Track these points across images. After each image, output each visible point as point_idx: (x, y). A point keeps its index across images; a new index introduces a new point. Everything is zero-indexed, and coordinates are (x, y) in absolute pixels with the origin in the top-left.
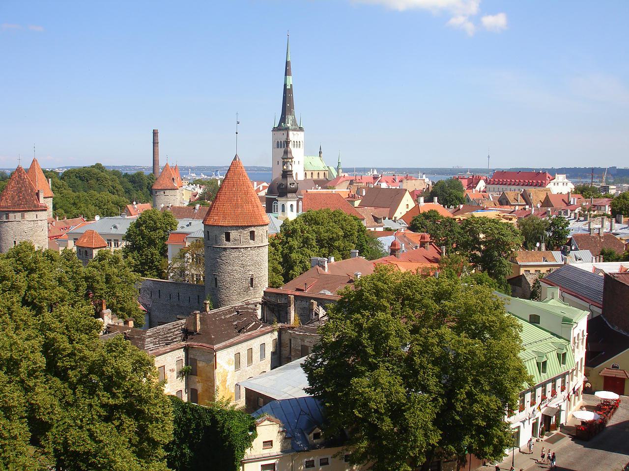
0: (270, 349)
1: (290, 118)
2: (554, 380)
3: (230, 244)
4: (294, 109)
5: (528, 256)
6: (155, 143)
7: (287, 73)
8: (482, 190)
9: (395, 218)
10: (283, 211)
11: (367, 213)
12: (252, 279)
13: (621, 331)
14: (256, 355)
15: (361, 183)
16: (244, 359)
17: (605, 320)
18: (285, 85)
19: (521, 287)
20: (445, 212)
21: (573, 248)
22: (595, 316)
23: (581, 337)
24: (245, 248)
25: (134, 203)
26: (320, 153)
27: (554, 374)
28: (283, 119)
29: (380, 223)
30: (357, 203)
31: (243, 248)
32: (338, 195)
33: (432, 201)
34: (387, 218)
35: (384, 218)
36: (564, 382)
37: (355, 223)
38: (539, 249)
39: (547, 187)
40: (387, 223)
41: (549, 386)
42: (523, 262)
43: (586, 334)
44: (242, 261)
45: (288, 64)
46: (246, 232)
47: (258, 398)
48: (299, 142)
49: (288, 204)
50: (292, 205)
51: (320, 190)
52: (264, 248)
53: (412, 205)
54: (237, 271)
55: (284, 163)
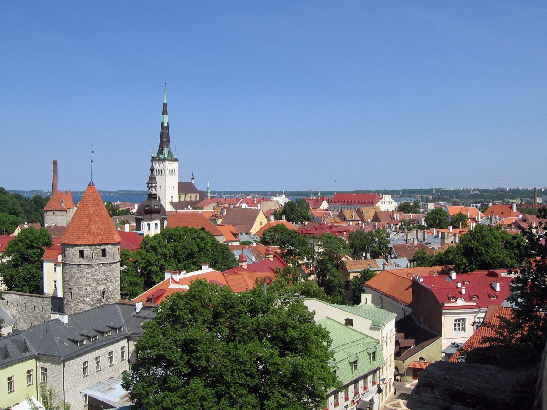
0: (117, 355)
1: (165, 151)
2: (365, 377)
3: (84, 261)
4: (169, 143)
5: (356, 264)
6: (55, 171)
7: (165, 112)
8: (325, 209)
9: (251, 233)
10: (149, 229)
11: (228, 229)
12: (104, 292)
13: (426, 328)
14: (105, 362)
15: (226, 204)
16: (91, 365)
17: (414, 318)
18: (163, 123)
19: (349, 291)
20: (291, 226)
21: (393, 256)
22: (407, 314)
23: (389, 335)
24: (98, 264)
25: (26, 223)
26: (193, 179)
27: (363, 371)
28: (160, 152)
29: (236, 238)
30: (219, 222)
31: (96, 264)
32: (201, 215)
33: (281, 219)
34: (244, 234)
35: (241, 234)
36: (374, 377)
37: (209, 240)
38: (366, 257)
39: (376, 205)
40: (244, 238)
41: (361, 383)
42: (351, 269)
43: (394, 332)
44: (94, 276)
45: (165, 105)
46: (99, 250)
47: (99, 405)
48: (174, 170)
49: (152, 223)
50: (156, 224)
51: (190, 209)
52: (116, 264)
53: (265, 222)
54: (90, 285)
55: (149, 188)
